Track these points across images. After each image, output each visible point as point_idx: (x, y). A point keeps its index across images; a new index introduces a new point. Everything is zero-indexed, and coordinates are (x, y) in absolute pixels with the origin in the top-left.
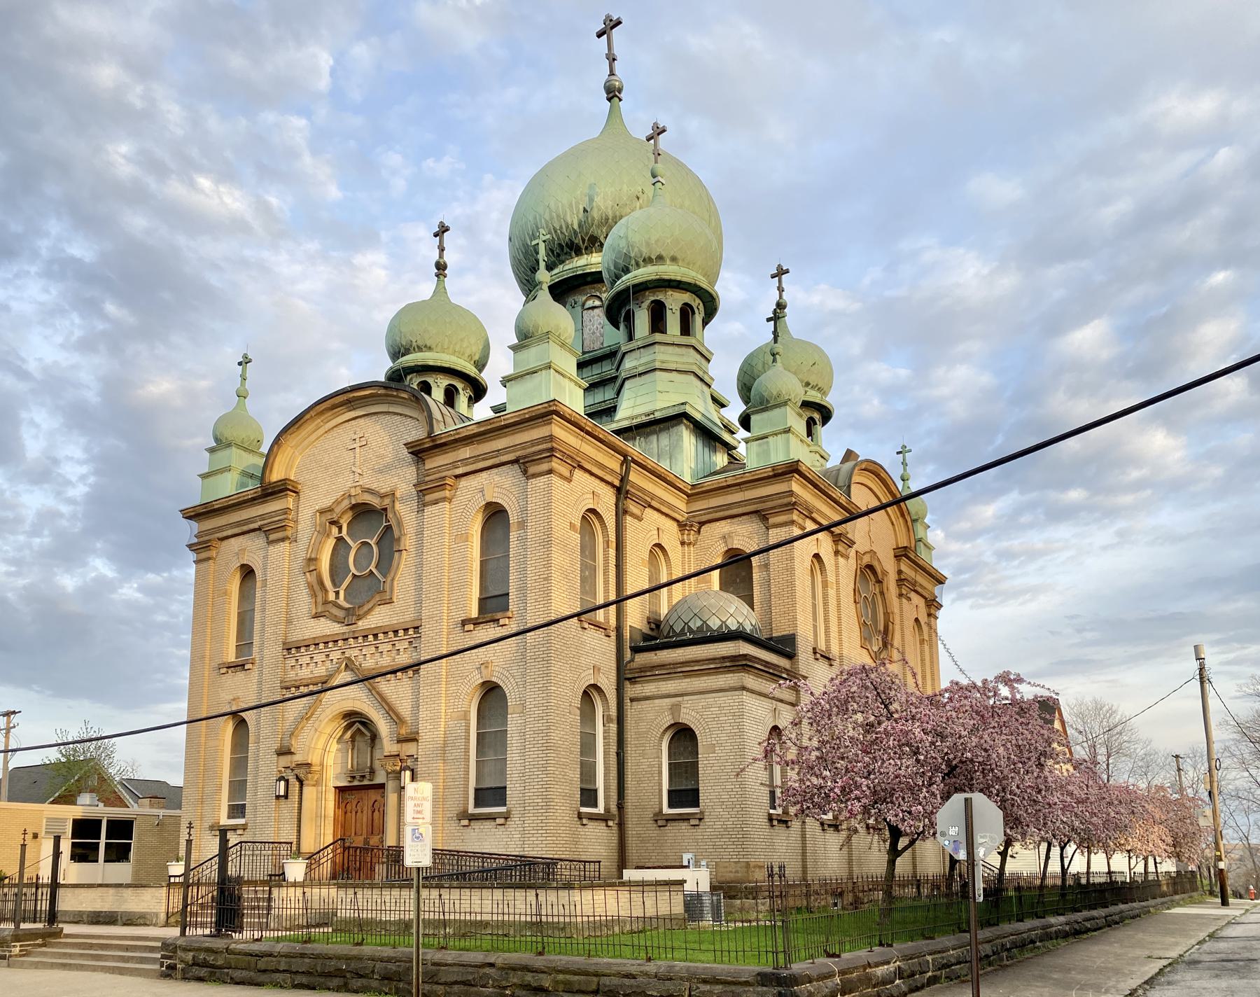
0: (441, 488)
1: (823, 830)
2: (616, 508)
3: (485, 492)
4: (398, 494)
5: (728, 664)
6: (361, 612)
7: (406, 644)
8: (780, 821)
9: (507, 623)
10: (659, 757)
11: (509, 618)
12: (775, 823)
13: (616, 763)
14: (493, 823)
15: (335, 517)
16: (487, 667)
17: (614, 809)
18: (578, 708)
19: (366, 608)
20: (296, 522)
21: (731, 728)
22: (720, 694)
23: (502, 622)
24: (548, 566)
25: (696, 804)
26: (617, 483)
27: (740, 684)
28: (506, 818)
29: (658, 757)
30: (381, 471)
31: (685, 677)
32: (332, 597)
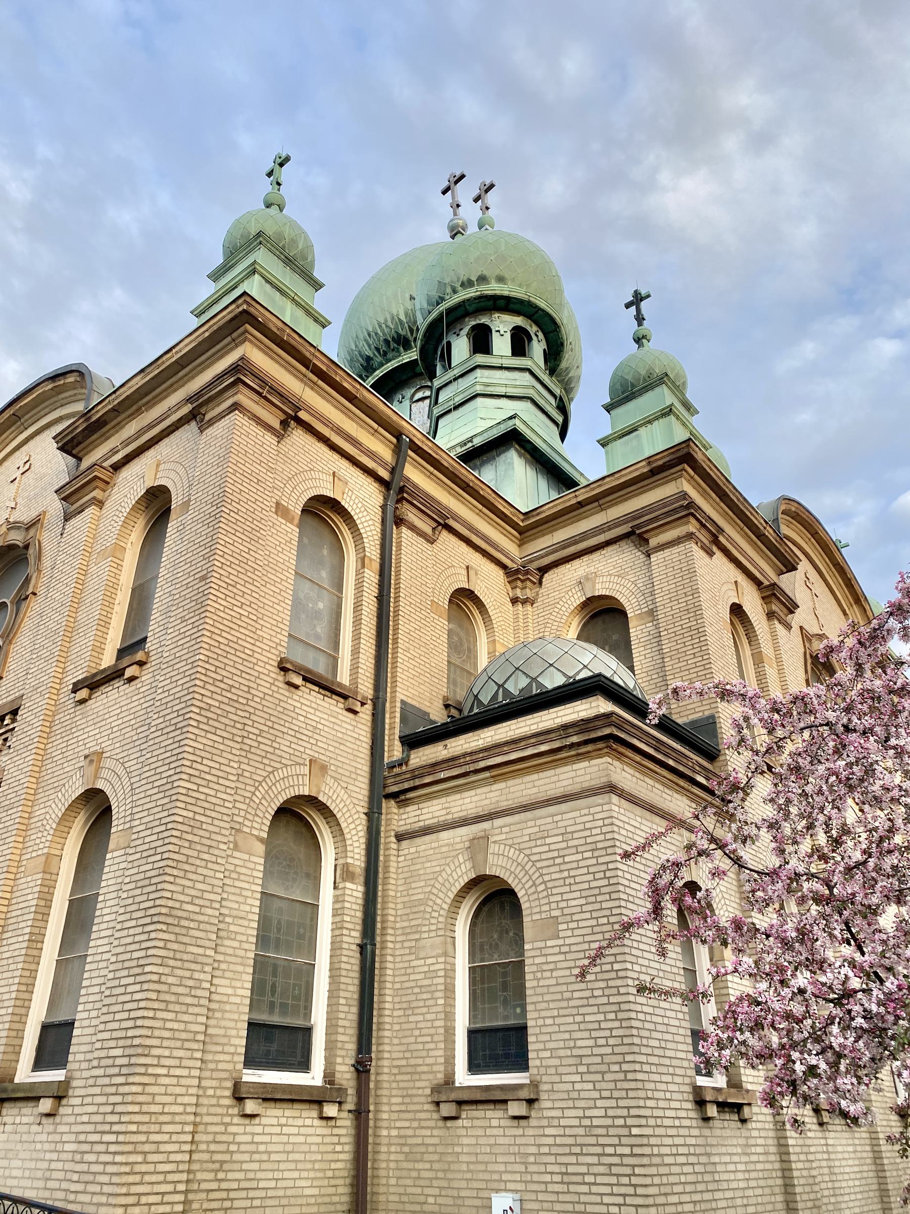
1: (821, 1124)
2: (383, 513)
5: (575, 739)
8: (723, 1106)
10: (448, 954)
11: (141, 664)
12: (712, 1110)
13: (357, 968)
17: (345, 1074)
18: (261, 840)
21: (591, 877)
22: (564, 807)
25: (520, 1062)
26: (384, 474)
27: (604, 780)
29: (445, 954)
31: (496, 779)
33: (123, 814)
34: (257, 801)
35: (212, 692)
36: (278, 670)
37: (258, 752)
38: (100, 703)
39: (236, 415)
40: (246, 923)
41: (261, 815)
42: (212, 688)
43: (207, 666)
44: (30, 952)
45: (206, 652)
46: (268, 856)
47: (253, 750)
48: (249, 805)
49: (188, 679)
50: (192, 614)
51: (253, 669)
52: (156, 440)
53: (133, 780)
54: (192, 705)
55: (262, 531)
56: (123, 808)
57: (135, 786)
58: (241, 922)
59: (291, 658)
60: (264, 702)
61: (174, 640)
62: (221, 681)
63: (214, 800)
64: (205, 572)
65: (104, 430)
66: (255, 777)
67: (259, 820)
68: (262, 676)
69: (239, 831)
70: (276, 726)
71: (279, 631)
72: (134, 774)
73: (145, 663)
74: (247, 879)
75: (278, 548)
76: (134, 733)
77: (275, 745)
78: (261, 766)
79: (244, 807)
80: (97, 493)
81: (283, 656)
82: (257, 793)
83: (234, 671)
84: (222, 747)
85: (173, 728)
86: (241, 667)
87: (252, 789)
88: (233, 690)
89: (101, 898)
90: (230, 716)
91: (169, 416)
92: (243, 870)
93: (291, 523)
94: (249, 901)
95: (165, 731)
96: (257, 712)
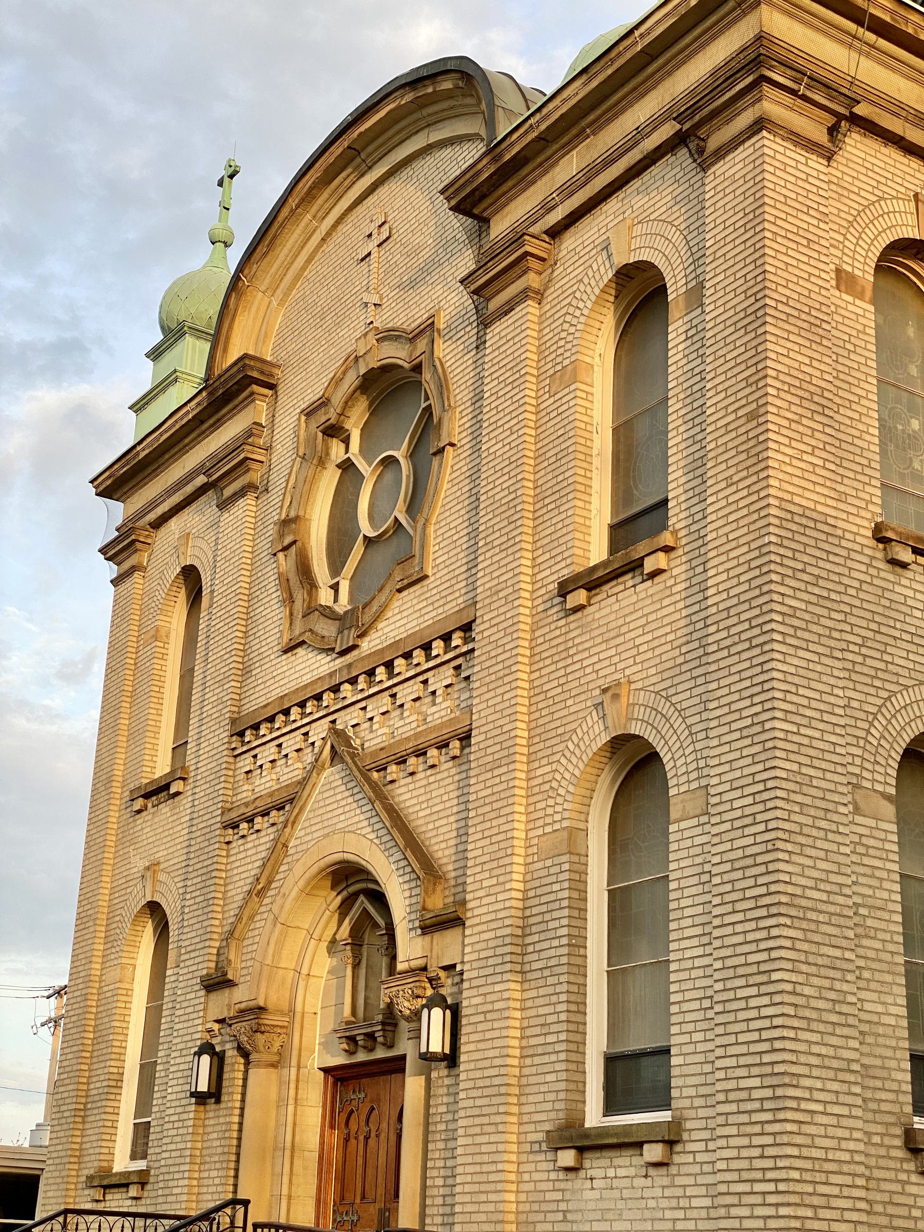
0: (517, 270)
3: (613, 248)
4: (441, 324)
6: (367, 618)
7: (447, 675)
9: (663, 565)
14: (637, 1160)
15: (332, 415)
16: (616, 697)
19: (375, 607)
20: (268, 449)
23: (649, 565)
24: (758, 380)
28: (670, 1143)
30: (413, 284)
32: (325, 597)
33: (684, 769)
34: (875, 743)
35: (794, 589)
36: (873, 543)
37: (865, 670)
38: (608, 610)
39: (768, 142)
40: (886, 916)
41: (883, 762)
42: (793, 583)
43: (782, 551)
44: (574, 960)
45: (777, 531)
46: (901, 821)
47: (858, 668)
48: (864, 748)
49: (757, 572)
50: (745, 473)
51: (839, 546)
52: (616, 185)
53: (689, 721)
54: (772, 611)
55: (825, 326)
56: (682, 760)
57: (694, 729)
58: (879, 914)
59: (894, 524)
60: (862, 595)
61: (720, 514)
62: (803, 571)
63: (821, 745)
64: (754, 405)
65: (524, 171)
66: (866, 707)
67: (882, 770)
68: (853, 555)
69: (857, 786)
70: (883, 629)
71: (867, 479)
72: (688, 713)
73: (673, 549)
74: (878, 853)
75: (848, 346)
76: (677, 652)
77: (887, 657)
78: (872, 691)
79: (859, 752)
80: (532, 280)
81: (879, 520)
82: (873, 731)
83: (818, 553)
84: (819, 668)
85: (746, 645)
86: (827, 547)
87: (866, 726)
88: (821, 583)
89: (673, 885)
90: (823, 621)
91: (637, 143)
92: (872, 842)
93: (862, 299)
94: (887, 885)
95: (734, 650)
96: (855, 611)
